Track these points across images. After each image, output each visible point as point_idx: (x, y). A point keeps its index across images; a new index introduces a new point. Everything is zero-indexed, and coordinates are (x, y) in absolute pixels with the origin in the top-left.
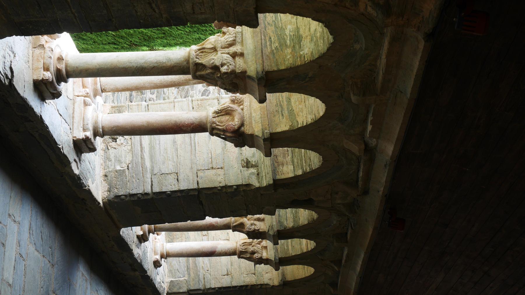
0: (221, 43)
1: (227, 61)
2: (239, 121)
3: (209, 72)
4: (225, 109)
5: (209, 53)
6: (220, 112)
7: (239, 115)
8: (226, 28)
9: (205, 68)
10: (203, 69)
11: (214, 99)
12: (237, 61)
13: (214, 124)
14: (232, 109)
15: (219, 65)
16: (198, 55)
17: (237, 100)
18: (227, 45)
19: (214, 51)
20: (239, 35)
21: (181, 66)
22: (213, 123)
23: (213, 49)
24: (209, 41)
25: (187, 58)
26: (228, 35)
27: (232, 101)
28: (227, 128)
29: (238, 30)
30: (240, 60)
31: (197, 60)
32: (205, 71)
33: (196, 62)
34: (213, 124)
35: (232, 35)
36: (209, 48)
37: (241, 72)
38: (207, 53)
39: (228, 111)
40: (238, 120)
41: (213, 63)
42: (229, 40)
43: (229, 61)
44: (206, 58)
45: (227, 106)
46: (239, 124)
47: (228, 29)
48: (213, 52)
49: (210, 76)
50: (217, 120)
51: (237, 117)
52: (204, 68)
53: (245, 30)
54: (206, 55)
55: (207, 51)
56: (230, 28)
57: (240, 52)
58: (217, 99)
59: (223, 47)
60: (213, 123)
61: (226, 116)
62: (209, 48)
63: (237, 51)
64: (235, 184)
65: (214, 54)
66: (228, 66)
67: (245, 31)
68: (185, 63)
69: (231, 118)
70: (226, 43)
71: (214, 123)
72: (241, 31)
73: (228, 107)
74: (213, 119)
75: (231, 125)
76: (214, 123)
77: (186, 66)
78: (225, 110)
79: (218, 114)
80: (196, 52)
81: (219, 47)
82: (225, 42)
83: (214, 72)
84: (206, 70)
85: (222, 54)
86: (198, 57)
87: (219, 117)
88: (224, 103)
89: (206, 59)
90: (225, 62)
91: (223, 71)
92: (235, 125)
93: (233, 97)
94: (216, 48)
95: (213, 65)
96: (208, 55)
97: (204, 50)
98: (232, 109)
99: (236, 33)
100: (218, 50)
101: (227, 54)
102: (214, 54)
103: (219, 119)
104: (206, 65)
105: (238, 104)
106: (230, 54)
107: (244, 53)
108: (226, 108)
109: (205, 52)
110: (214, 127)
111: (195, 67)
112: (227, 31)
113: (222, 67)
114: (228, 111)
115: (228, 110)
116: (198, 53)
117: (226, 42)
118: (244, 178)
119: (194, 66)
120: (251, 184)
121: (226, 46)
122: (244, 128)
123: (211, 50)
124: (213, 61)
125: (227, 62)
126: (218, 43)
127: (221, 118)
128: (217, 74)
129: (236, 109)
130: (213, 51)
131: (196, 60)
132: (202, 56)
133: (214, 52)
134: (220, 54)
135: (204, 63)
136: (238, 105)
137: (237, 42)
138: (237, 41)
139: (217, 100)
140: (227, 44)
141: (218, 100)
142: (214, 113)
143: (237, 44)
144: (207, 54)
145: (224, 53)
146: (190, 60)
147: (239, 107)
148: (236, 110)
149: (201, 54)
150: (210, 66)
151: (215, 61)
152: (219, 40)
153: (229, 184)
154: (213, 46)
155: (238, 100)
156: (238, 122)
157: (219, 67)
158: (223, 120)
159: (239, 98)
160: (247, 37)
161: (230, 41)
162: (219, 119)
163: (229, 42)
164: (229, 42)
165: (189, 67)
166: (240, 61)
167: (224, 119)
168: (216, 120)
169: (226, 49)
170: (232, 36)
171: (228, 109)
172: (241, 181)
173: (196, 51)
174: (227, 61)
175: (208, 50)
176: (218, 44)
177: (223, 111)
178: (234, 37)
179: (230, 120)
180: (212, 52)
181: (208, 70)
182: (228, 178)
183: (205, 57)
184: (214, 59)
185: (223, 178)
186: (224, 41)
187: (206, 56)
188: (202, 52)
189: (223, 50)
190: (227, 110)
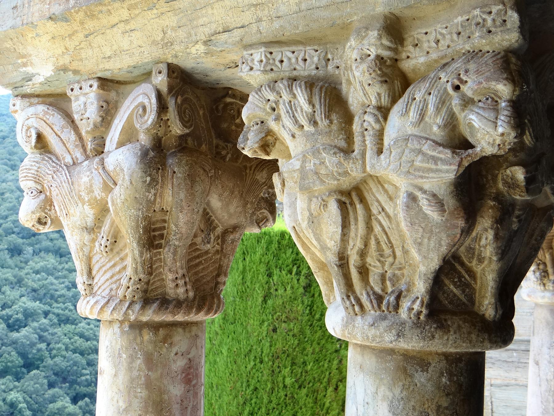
0: (316, 152)
1: (431, 109)
3: (490, 235)
5: (369, 228)
6: (541, 267)
8: (241, 136)
9: (462, 264)
10: (463, 272)
12: (434, 56)
15: (458, 159)
16: (380, 299)
18: (334, 117)
19: (362, 200)
20: (282, 61)
21: (439, 407)
23: (352, 204)
24: (304, 225)
25: (391, 365)
26: (278, 118)
29: (256, 65)
30: (428, 43)
31: (405, 304)
32: (481, 260)
33: (419, 313)
35: (279, 93)
36: (345, 225)
37: (519, 12)
38: (373, 242)
41: (440, 204)
42: (307, 108)
43: (432, 100)
44: (399, 253)
47: (250, 120)
48: (367, 209)
49: (516, 232)
52: (459, 267)
53: (259, 20)
54: (379, 249)
55: (359, 244)
56: (245, 114)
57: (380, 37)
59: (342, 144)
62: (339, 230)
63: (372, 57)
65: (382, 198)
66: (467, 103)
67: (264, 26)
68: (421, 378)
70: (323, 123)
72: (263, 49)
77: (442, 374)
79: (548, 274)
80: (361, 306)
81: (340, 164)
82: (312, 129)
83: (492, 203)
84: (471, 259)
85: (387, 141)
86: (392, 299)
89: (406, 252)
90: (439, 121)
91: (500, 130)
94: (346, 183)
95: (450, 202)
96: (383, 238)
97: (354, 260)
99: (272, 75)
100: (356, 174)
101: (385, 118)
102: (382, 198)
104: (444, 249)
106: (385, 101)
107: (387, 11)
109: (363, 254)
111: (453, 322)
112: (256, 127)
113: (472, 147)
116: (364, 299)
117: (315, 123)
119: (443, 327)
121: (334, 127)
123: (356, 219)
124: (424, 202)
125: (438, 110)
126: (317, 173)
128: (512, 184)
130: (359, 206)
131: (410, 309)
132: (388, 275)
133: (369, 198)
134: (382, 156)
135: (435, 263)
137: (321, 73)
138: (314, 72)
140: (328, 117)
142: (544, 285)
143: (330, 67)
144: (378, 243)
145: (380, 135)
146: (404, 345)
149: (374, 280)
150: (455, 227)
151: (426, 187)
152: (303, 167)
154: (333, 207)
157: (466, 164)
160: (295, 8)
161: (311, 102)
163: (314, 106)
164: (314, 106)
165: (446, 356)
166: (432, 37)
169: (356, 127)
170: (286, 97)
173: (357, 308)
174: (431, 109)
175: (352, 234)
176: (323, 171)
178: (290, 87)
180: (369, 216)
181: (478, 239)
183: (395, 257)
184: (412, 198)
186: (308, 136)
187: (387, 251)
188: (364, 271)
189: (357, 147)
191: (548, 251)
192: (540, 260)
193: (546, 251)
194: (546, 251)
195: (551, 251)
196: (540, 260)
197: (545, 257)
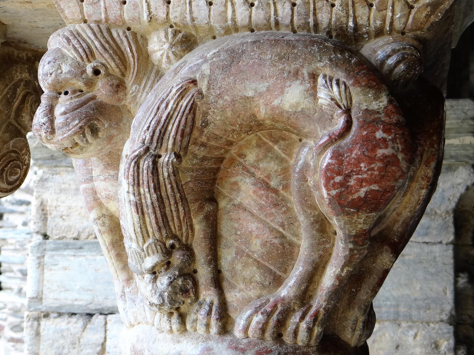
2: (305, 72)
4: (160, 199)
7: (244, 62)
11: (38, 334)
13: (290, 327)
14: (172, 129)
17: (90, 84)
22: (278, 337)
27: (94, 131)
28: (362, 192)
34: (288, 338)
39: (186, 178)
40: (296, 74)
45: (137, 183)
46: (340, 75)
50: (253, 293)
51: (262, 87)
58: (38, 319)
60: (278, 337)
61: (222, 204)
64: (451, 278)
69: (251, 157)
71: (281, 323)
73: (146, 164)
74: (238, 332)
75: (337, 156)
76: (281, 323)
78: (170, 208)
79: (196, 284)
87: (226, 273)
88: (93, 215)
92: (348, 111)
93: (59, 110)
98: (172, 129)
103: (247, 273)
105: (130, 80)
108: (157, 188)
110: (317, 330)
114: (186, 178)
115: (176, 172)
118: (426, 234)
120: (458, 204)
122: (379, 32)
127: (239, 253)
129: (182, 94)
136: (138, 80)
139: (44, 322)
141: (47, 316)
142: (182, 318)
147: (159, 74)
148: (193, 91)
153: (449, 306)
155: (89, 70)
156: (314, 77)
158: (267, 236)
159: (71, 54)
162: (247, 273)
167: (253, 226)
168: (248, 301)
171: (164, 172)
172: (437, 249)
177: (174, 226)
179: (273, 166)
182: (419, 308)
185: (415, 330)
190: (179, 187)
191: (201, 208)
192: (174, 237)
193: (194, 207)
194: (194, 207)
195: (208, 208)
196: (174, 237)
197: (192, 227)
